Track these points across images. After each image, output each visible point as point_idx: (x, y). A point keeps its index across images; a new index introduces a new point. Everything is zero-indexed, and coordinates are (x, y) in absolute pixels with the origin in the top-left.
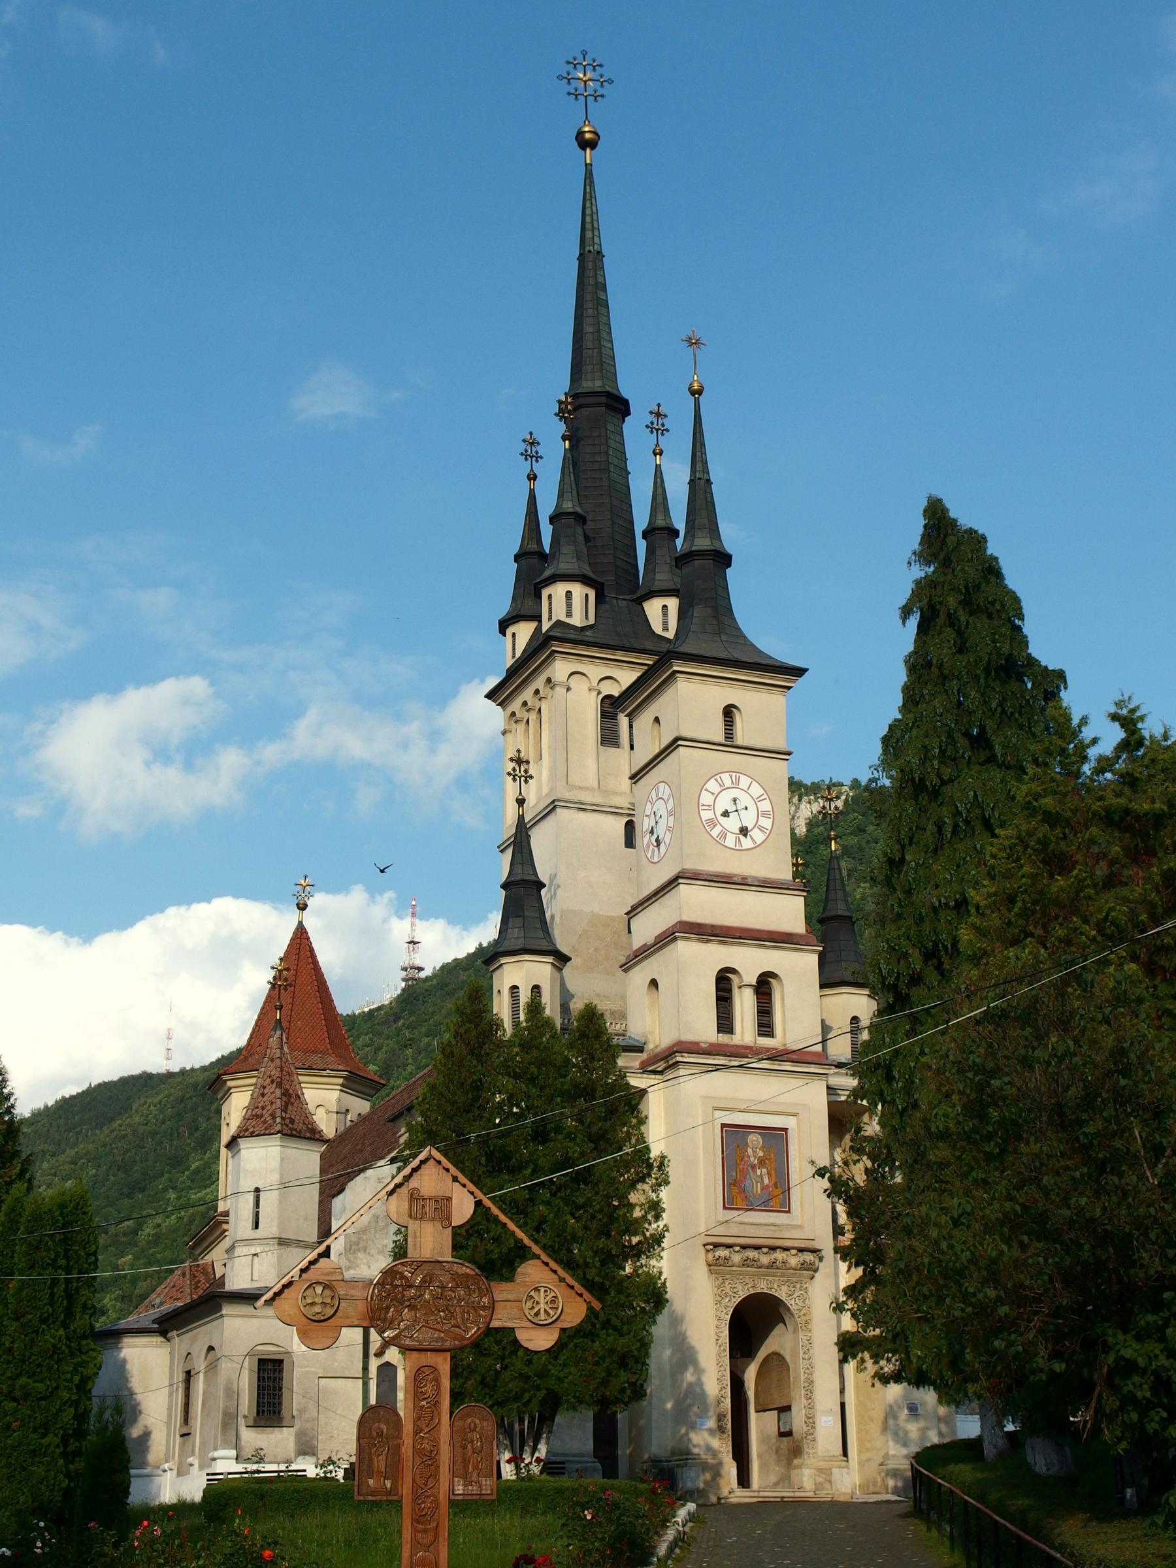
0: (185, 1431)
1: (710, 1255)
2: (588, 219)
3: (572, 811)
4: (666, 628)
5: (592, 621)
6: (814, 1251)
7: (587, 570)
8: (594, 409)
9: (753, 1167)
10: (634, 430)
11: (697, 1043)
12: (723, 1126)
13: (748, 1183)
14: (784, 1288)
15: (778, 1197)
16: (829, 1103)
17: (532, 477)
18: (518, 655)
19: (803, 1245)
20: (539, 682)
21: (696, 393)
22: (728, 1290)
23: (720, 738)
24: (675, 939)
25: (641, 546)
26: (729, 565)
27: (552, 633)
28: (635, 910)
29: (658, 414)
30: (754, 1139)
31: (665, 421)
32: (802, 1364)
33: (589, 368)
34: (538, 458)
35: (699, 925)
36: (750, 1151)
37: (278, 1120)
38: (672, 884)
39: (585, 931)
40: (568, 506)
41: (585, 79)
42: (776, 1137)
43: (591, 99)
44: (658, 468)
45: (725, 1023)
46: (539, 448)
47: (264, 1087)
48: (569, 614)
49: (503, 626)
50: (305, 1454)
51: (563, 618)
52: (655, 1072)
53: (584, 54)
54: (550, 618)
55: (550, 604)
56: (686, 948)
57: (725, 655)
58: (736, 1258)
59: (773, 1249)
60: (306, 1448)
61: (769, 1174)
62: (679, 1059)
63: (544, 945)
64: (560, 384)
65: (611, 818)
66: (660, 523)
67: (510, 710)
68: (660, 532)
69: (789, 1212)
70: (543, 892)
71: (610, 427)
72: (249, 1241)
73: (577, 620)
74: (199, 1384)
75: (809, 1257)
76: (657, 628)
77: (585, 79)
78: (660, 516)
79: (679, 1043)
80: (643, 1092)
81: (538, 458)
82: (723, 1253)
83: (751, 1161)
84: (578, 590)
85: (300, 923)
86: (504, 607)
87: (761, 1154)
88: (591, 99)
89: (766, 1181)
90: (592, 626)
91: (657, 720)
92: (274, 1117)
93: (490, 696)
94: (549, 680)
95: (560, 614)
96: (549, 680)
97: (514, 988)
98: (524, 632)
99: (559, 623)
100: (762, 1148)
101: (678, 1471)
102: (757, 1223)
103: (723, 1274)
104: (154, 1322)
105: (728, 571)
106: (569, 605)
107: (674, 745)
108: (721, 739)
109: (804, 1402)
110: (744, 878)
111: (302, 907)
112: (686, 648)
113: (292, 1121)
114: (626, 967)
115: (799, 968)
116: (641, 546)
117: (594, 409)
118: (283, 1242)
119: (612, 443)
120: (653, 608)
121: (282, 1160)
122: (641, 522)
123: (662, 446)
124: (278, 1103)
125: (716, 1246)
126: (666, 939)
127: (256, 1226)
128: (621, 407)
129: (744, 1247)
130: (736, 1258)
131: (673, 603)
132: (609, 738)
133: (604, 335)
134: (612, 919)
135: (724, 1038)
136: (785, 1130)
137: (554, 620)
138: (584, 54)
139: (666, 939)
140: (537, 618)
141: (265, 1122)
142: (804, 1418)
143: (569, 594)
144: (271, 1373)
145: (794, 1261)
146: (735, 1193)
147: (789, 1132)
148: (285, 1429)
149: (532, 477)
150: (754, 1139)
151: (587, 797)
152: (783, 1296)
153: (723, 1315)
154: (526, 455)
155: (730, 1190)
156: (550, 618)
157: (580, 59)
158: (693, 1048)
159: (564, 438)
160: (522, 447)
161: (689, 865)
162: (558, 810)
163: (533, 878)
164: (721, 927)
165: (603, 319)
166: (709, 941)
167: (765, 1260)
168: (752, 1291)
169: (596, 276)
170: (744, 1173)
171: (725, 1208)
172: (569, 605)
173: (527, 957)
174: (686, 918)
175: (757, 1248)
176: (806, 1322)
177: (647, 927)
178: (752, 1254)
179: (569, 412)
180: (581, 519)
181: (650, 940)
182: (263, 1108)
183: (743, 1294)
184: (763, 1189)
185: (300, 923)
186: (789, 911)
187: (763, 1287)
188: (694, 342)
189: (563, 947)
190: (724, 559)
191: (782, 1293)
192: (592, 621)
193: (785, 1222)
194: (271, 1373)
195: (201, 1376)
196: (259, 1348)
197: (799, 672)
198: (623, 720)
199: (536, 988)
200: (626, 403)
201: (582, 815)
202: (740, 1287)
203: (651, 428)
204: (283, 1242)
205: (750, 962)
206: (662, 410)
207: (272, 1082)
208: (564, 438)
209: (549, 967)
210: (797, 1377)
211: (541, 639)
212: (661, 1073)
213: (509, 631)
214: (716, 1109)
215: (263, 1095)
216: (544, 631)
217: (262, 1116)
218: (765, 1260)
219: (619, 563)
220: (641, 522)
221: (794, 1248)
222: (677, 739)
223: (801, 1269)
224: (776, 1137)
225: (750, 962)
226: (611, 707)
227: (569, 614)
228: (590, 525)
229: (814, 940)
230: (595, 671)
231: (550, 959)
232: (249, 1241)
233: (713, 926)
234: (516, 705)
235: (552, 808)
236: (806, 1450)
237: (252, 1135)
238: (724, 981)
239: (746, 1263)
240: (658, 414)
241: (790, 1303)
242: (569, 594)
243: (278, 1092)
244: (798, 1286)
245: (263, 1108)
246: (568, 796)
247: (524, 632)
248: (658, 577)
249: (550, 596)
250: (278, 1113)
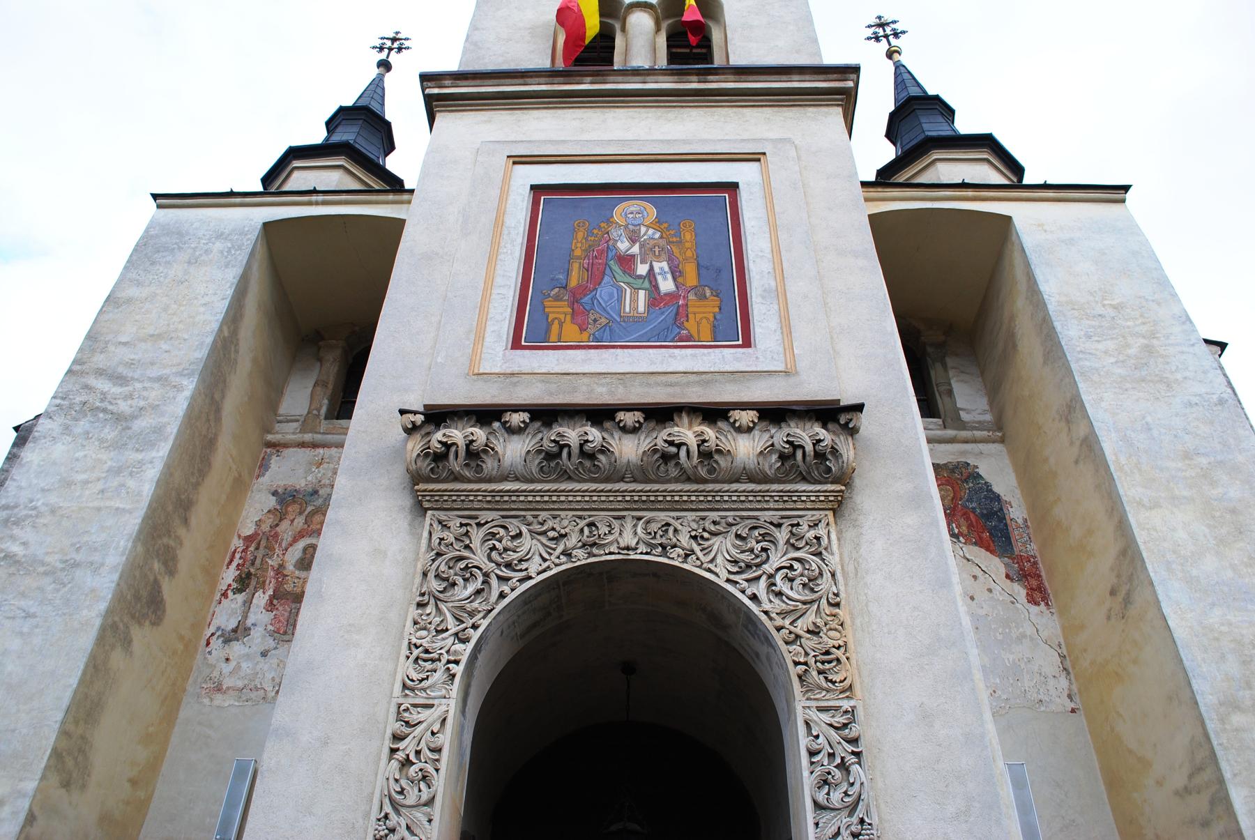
1: (415, 446)
6: (832, 414)
12: (538, 190)
14: (724, 546)
61: (676, 273)
89: (666, 285)
103: (469, 512)
147: (744, 196)
152: (720, 575)
167: (629, 449)
168: (582, 558)
170: (596, 274)
202: (527, 543)
214: (519, 160)
218: (628, 449)
221: (744, 406)
244: (782, 535)
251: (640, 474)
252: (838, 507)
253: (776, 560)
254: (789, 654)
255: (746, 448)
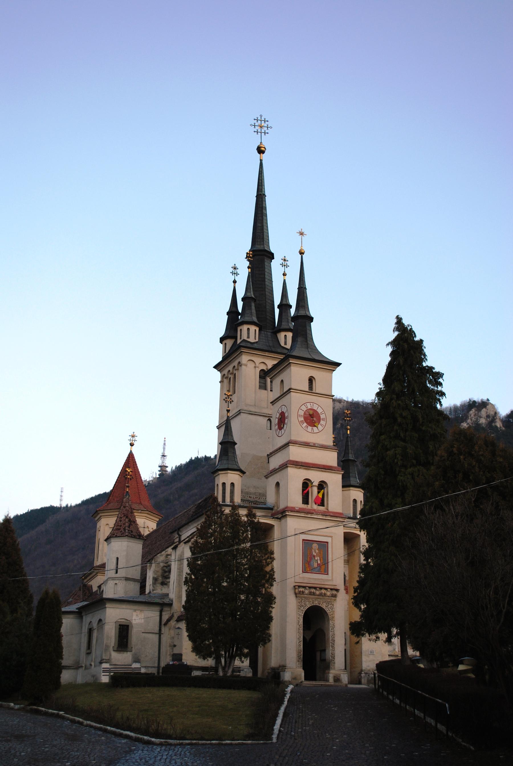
0: (88, 651)
1: (297, 591)
2: (260, 181)
3: (247, 414)
4: (286, 344)
5: (257, 340)
7: (255, 319)
8: (260, 256)
9: (314, 556)
10: (276, 266)
11: (294, 508)
12: (303, 540)
13: (312, 562)
15: (323, 568)
16: (344, 533)
17: (235, 282)
18: (227, 352)
19: (332, 587)
20: (235, 363)
21: (302, 253)
22: (303, 604)
23: (307, 390)
24: (287, 467)
25: (277, 311)
26: (312, 321)
27: (241, 344)
28: (269, 456)
29: (285, 260)
30: (315, 546)
31: (287, 263)
32: (331, 633)
33: (259, 240)
34: (237, 274)
35: (297, 462)
36: (313, 551)
37: (127, 531)
38: (286, 445)
39: (250, 461)
40: (249, 295)
41: (261, 126)
42: (324, 546)
43: (263, 134)
44: (284, 281)
45: (306, 500)
46: (238, 271)
47: (121, 518)
48: (248, 337)
49: (222, 340)
50: (136, 662)
51: (246, 338)
52: (277, 518)
53: (261, 116)
54: (241, 338)
55: (241, 333)
56: (291, 471)
57: (310, 357)
58: (307, 592)
59: (321, 588)
60: (137, 660)
62: (287, 513)
63: (236, 467)
64: (247, 246)
65: (261, 418)
66: (284, 302)
67: (223, 373)
68: (284, 306)
69: (327, 574)
70: (236, 446)
71: (266, 264)
72: (113, 579)
73: (252, 339)
74: (95, 634)
75: (334, 592)
76: (282, 344)
77: (261, 126)
78: (284, 300)
79: (287, 507)
80: (273, 526)
81: (237, 274)
82: (301, 589)
83: (314, 555)
84: (253, 328)
85: (131, 451)
86: (222, 332)
87: (317, 551)
88: (263, 134)
89: (319, 562)
90: (257, 342)
91: (282, 381)
92: (125, 529)
93: (215, 367)
94: (239, 363)
95: (245, 337)
96: (239, 363)
97: (224, 484)
98: (229, 343)
99: (244, 340)
100: (318, 549)
101: (282, 673)
102: (314, 578)
103: (301, 597)
104: (77, 609)
105: (312, 323)
106: (248, 334)
107: (289, 390)
108: (307, 390)
109: (331, 648)
110: (314, 444)
111: (132, 445)
112: (294, 353)
113: (132, 532)
114: (267, 477)
115: (334, 480)
116: (277, 311)
117: (260, 256)
118: (127, 579)
119: (266, 270)
120: (281, 336)
121: (128, 546)
122: (277, 301)
123: (286, 272)
124: (127, 524)
125: (299, 587)
126: (284, 466)
127: (117, 573)
128: (271, 256)
129: (310, 588)
130: (307, 592)
131: (290, 335)
132: (263, 386)
133: (265, 227)
134: (261, 457)
135: (305, 506)
136: (327, 543)
137: (242, 339)
138: (261, 116)
139: (284, 466)
140: (236, 338)
141: (121, 532)
142: (331, 654)
143: (248, 329)
144: (124, 631)
145: (328, 593)
146: (307, 566)
148: (129, 653)
149: (235, 282)
150: (315, 546)
151: (253, 409)
152: (324, 607)
153: (301, 614)
154: (232, 273)
155: (305, 565)
156: (241, 338)
157: (259, 119)
158: (293, 510)
159: (249, 268)
160: (232, 270)
161: (293, 438)
162: (242, 414)
163: (232, 441)
164: (305, 463)
165: (264, 221)
166: (300, 468)
167: (318, 592)
169: (262, 204)
170: (311, 559)
171: (303, 572)
172: (248, 334)
173: (229, 472)
174: (291, 459)
175: (315, 588)
176: (333, 617)
177: (276, 462)
178: (313, 590)
179: (251, 257)
180: (254, 300)
181: (277, 467)
182: (121, 526)
183: (309, 606)
184: (318, 564)
185: (131, 451)
186: (331, 458)
187: (316, 603)
188: (302, 234)
189: (243, 469)
190: (311, 319)
191: (324, 606)
192: (257, 340)
193: (326, 578)
194: (124, 631)
195: (96, 630)
196: (120, 620)
197: (338, 364)
198: (269, 380)
199: (232, 484)
200: (272, 254)
201: (250, 416)
202: (307, 603)
203: (282, 265)
204: (127, 579)
205: (316, 477)
206: (287, 258)
207: (124, 516)
208: (249, 268)
209: (238, 475)
210: (328, 639)
211: (237, 347)
212: (280, 519)
213: (224, 342)
215: (121, 521)
216: (238, 343)
217: (120, 529)
218: (318, 592)
219: (268, 317)
220: (277, 301)
222: (290, 389)
223: (332, 597)
224: (324, 546)
225: (316, 477)
226: (264, 374)
227: (248, 337)
228: (258, 302)
229: (340, 468)
230: (258, 360)
231: (238, 473)
232: (113, 579)
233: (302, 462)
234: (225, 372)
235: (239, 413)
236: (331, 667)
237: (116, 536)
238: (306, 484)
239: (310, 593)
240: (285, 260)
241: (326, 610)
242: (248, 329)
243: (127, 520)
245: (121, 526)
246: (245, 408)
247: (229, 343)
248: (283, 323)
249: (241, 330)
250: (127, 528)
251: (318, 595)
252: (335, 600)
253: (330, 606)
254: (330, 616)
255: (328, 593)
